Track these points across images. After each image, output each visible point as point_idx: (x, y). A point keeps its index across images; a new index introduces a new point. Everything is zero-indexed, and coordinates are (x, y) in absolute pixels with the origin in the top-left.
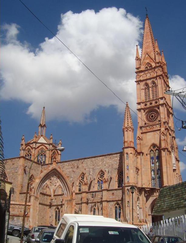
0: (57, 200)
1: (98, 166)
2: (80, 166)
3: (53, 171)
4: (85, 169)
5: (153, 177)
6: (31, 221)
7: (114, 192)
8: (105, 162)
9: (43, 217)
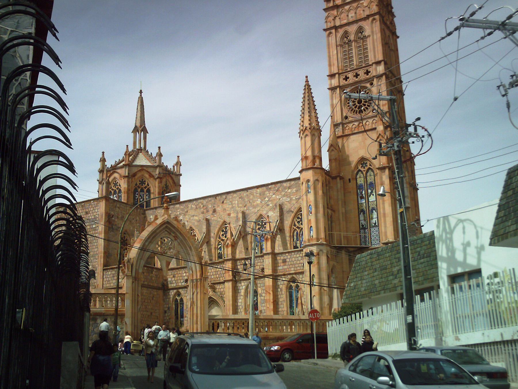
0: (176, 279)
1: (254, 207)
2: (218, 209)
3: (164, 226)
4: (229, 215)
5: (363, 226)
6: (128, 323)
7: (285, 258)
8: (267, 199)
9: (151, 313)
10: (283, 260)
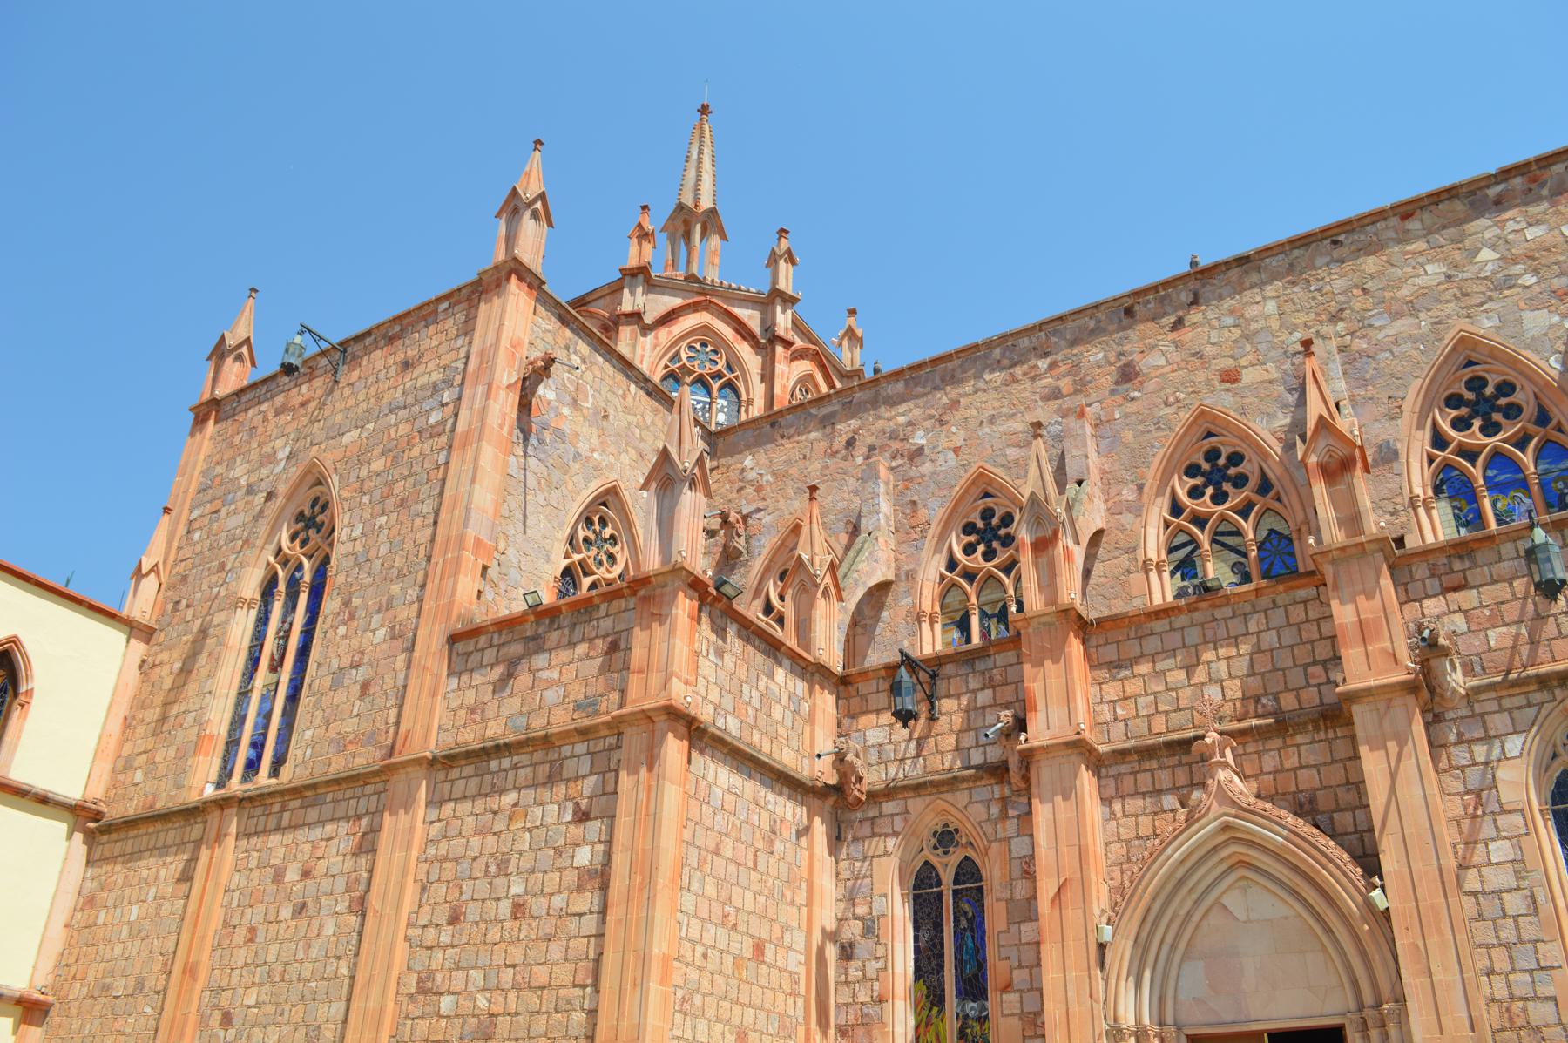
4: (1230, 377)
8: (1486, 254)
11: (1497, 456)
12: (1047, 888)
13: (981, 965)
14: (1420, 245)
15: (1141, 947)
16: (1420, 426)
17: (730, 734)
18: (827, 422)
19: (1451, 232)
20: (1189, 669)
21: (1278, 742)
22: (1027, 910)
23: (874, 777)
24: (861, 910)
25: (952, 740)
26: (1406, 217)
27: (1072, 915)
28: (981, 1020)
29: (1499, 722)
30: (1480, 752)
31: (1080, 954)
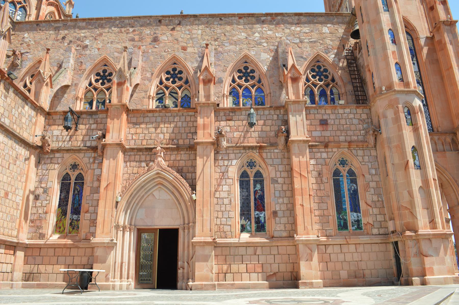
2: (163, 38)
4: (184, 49)
7: (325, 117)
8: (257, 35)
10: (321, 120)
11: (247, 89)
12: (103, 184)
13: (80, 205)
14: (241, 27)
15: (128, 204)
16: (230, 76)
17: (5, 124)
18: (57, 29)
19: (250, 26)
20: (156, 128)
21: (176, 152)
22: (97, 190)
23: (54, 145)
24: (43, 185)
25: (81, 138)
26: (240, 18)
27: (110, 193)
28: (78, 220)
29: (232, 156)
30: (226, 163)
31: (110, 203)
